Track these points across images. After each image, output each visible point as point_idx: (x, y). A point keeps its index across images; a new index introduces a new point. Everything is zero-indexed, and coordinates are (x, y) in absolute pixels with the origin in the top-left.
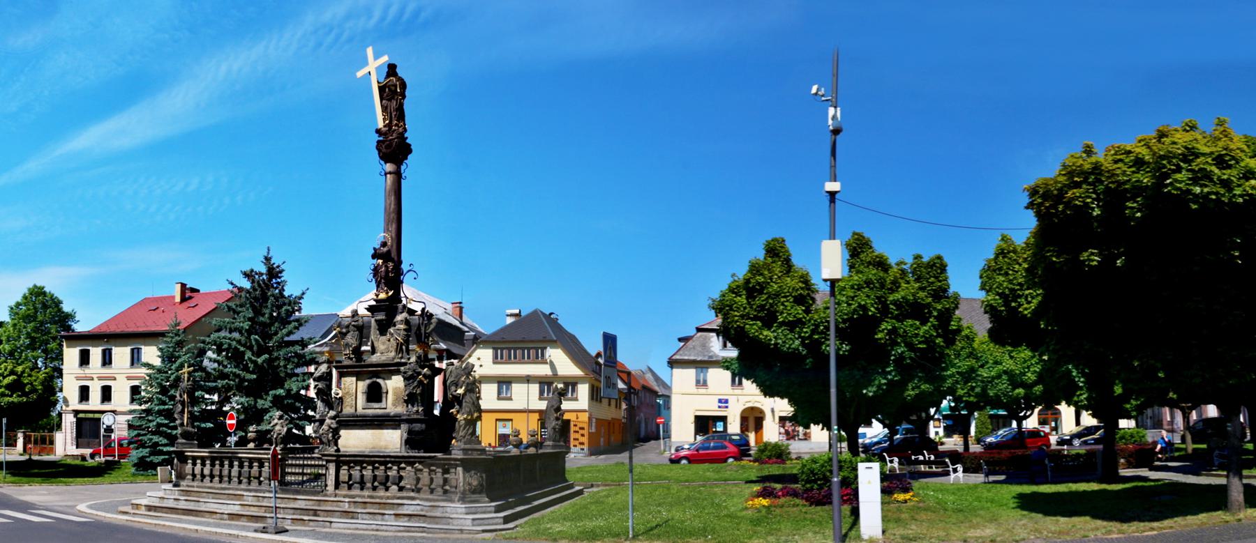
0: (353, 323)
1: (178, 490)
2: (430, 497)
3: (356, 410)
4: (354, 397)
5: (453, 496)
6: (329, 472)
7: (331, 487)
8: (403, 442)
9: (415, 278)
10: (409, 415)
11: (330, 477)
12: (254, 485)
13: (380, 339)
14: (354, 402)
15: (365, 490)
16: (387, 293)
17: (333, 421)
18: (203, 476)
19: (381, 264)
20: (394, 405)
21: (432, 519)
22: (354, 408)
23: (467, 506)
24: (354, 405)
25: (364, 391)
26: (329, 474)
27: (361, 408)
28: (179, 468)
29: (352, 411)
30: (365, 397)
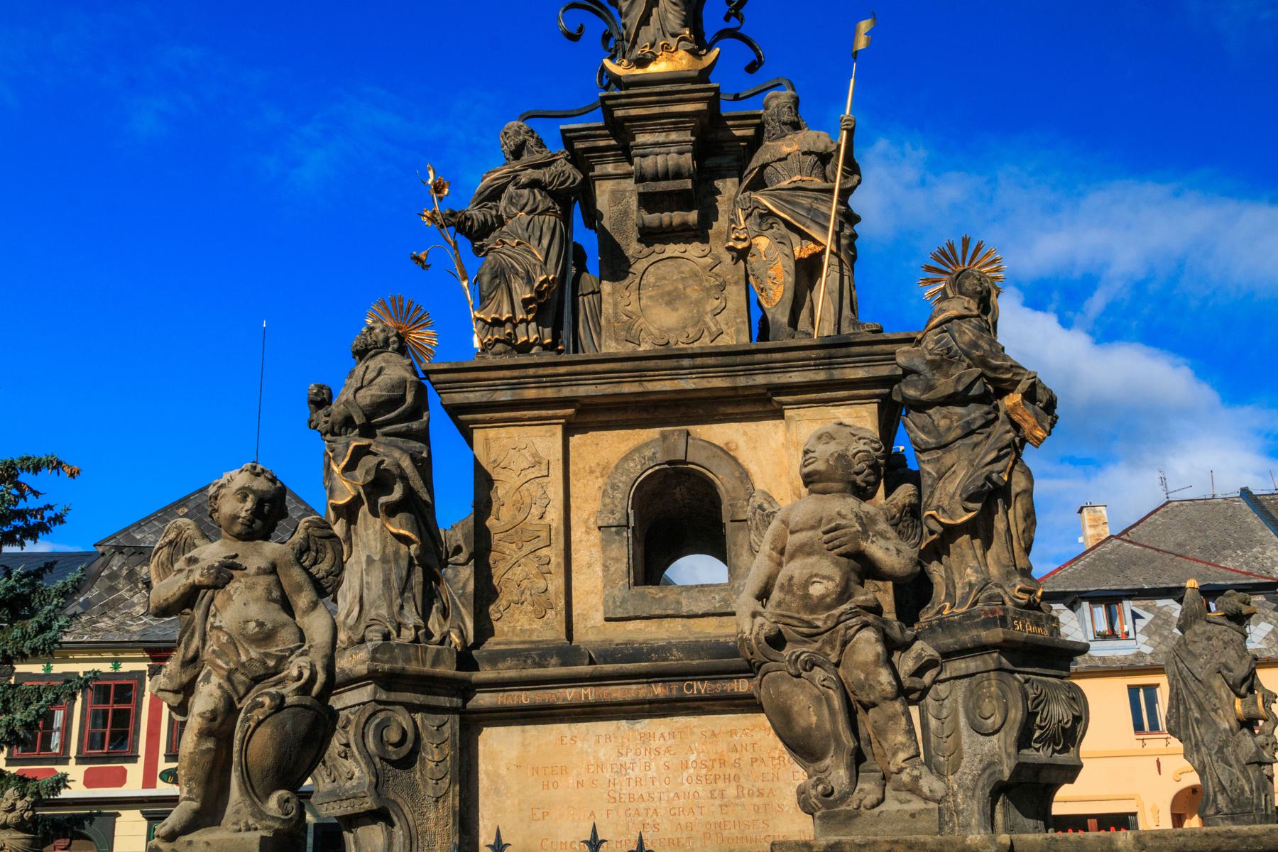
3: (569, 635)
4: (554, 554)
13: (650, 278)
14: (557, 583)
24: (562, 603)
25: (618, 517)
27: (598, 618)
29: (549, 630)
30: (621, 552)
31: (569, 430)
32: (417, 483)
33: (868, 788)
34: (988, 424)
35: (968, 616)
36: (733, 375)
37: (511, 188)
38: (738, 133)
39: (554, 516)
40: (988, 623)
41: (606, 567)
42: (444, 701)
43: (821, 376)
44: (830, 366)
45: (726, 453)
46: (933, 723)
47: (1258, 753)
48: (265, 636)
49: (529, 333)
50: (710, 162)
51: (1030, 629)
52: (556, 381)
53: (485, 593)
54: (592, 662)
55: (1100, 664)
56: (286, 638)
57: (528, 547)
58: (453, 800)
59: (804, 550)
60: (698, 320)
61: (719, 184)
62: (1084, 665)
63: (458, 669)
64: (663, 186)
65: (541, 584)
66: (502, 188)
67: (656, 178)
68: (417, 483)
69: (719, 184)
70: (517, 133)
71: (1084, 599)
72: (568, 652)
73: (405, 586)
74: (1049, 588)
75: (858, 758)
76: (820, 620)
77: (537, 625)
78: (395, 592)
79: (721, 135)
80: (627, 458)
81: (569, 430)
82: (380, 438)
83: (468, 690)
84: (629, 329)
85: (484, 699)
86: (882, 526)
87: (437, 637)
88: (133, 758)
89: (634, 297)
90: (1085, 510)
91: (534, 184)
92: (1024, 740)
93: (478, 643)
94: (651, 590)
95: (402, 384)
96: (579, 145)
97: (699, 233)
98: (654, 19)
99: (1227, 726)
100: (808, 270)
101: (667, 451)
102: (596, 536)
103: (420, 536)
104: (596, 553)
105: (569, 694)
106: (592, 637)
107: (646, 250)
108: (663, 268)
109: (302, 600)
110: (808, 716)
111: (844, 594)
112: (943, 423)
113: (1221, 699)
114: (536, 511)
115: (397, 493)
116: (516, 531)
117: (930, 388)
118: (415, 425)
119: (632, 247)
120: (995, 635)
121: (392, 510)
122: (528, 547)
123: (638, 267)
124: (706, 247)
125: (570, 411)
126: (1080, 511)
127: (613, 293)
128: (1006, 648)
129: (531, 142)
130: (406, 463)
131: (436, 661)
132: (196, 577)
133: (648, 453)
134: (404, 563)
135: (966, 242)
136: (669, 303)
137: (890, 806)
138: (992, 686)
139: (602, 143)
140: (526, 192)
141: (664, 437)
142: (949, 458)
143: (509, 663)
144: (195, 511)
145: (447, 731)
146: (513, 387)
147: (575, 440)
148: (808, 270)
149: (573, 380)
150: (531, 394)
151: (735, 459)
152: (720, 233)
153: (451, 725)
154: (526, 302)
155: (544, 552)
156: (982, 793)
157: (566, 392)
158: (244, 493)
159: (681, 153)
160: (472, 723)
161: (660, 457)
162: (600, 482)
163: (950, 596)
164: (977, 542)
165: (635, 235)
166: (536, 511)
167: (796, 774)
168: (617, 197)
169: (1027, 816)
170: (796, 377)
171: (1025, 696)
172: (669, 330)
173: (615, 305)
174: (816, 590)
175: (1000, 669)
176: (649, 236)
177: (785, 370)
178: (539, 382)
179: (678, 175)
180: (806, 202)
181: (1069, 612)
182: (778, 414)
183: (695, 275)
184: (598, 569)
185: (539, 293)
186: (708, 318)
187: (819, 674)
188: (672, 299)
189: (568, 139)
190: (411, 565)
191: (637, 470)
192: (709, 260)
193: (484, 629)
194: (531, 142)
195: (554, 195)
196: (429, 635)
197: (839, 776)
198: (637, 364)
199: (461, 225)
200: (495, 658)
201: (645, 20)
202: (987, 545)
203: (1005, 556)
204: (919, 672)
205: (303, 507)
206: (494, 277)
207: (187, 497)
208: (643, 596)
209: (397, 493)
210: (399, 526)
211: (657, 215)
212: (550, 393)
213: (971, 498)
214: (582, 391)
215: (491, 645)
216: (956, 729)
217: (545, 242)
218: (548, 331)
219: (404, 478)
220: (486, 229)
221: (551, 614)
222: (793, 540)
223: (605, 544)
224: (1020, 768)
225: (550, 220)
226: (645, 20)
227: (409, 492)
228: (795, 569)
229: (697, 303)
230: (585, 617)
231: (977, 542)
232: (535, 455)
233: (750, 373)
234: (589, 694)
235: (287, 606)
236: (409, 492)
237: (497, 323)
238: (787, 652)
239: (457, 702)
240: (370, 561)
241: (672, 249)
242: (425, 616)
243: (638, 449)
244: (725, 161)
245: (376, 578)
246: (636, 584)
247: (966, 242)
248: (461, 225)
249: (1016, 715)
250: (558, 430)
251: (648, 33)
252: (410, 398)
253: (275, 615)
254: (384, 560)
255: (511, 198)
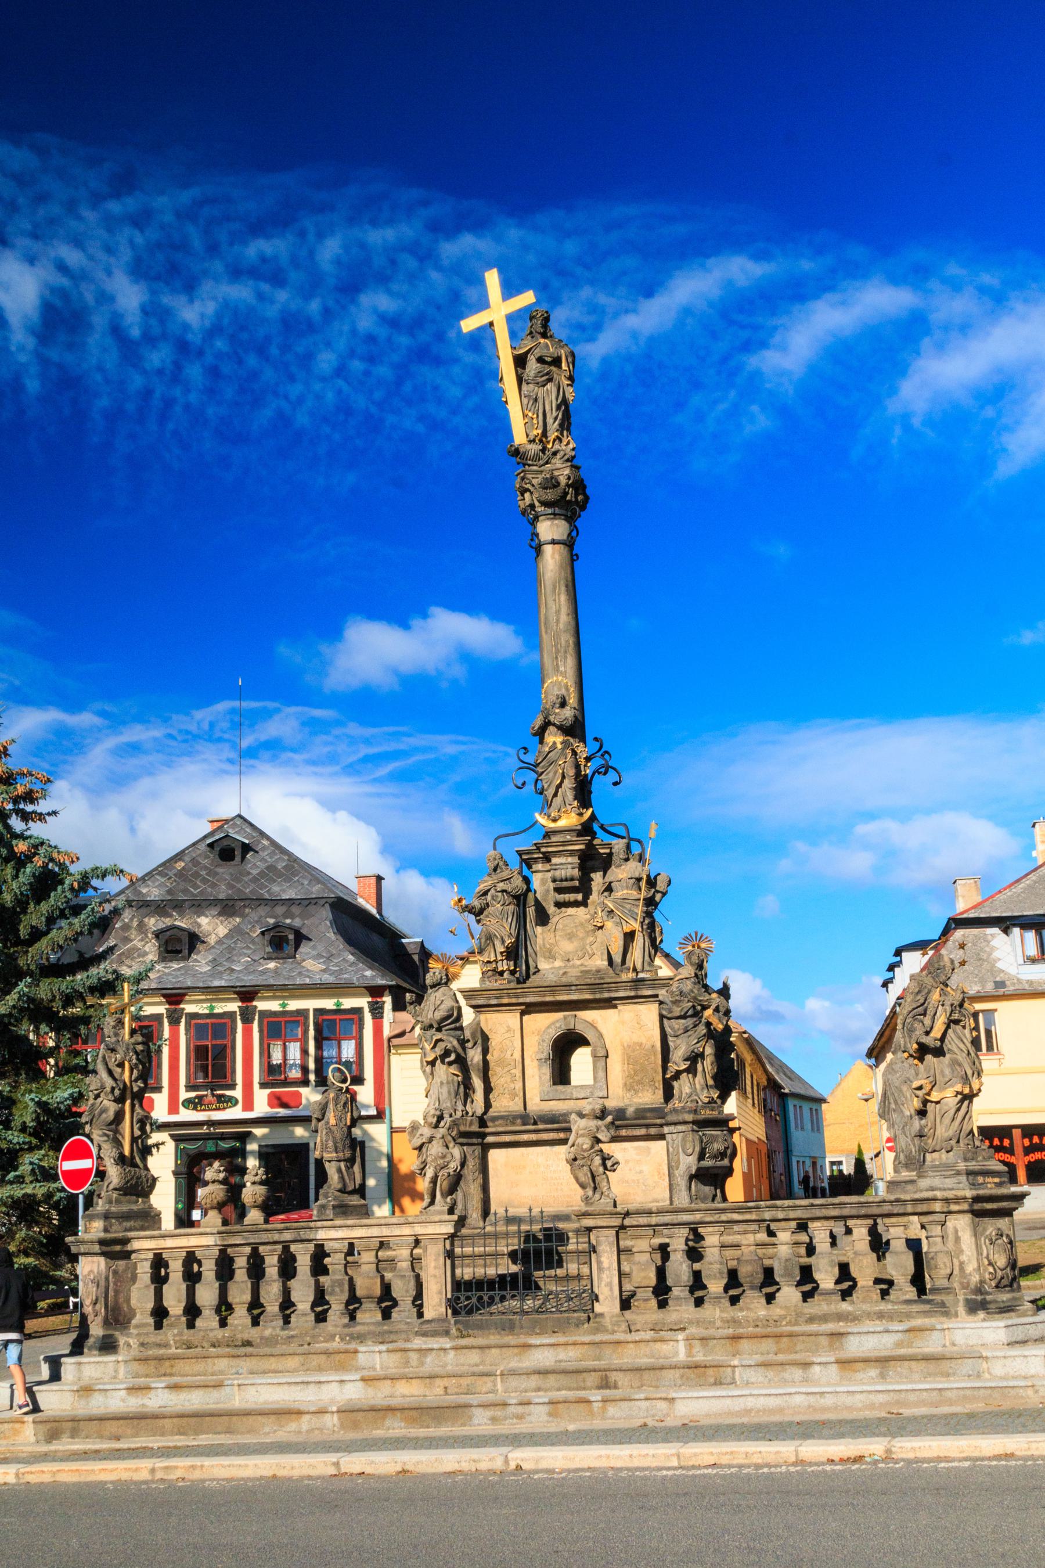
0: (501, 886)
1: (126, 1362)
2: (883, 1306)
4: (518, 1072)
5: (947, 1299)
6: (599, 1262)
7: (608, 1305)
8: (682, 1182)
9: (616, 784)
10: (695, 1111)
11: (604, 1276)
12: (369, 1316)
13: (560, 926)
15: (706, 1305)
16: (581, 814)
17: (600, 1123)
18: (192, 1311)
19: (559, 746)
20: (629, 1087)
21: (932, 1366)
22: (519, 1101)
23: (1010, 1322)
25: (545, 1055)
26: (600, 1269)
27: (537, 1100)
28: (111, 1293)
29: (516, 1106)
30: (547, 1071)
31: (523, 1013)
32: (460, 1050)
33: (597, 1196)
34: (695, 1026)
35: (683, 1108)
36: (594, 993)
37: (492, 891)
38: (602, 851)
39: (517, 1055)
40: (690, 1112)
41: (540, 1078)
42: (475, 1141)
43: (632, 994)
44: (636, 989)
45: (593, 1026)
46: (671, 1149)
47: (920, 1131)
48: (444, 1157)
49: (504, 966)
50: (589, 864)
51: (708, 1112)
52: (517, 997)
53: (488, 1089)
54: (535, 1123)
55: (1027, 987)
56: (449, 1157)
57: (506, 1069)
58: (480, 1181)
59: (583, 1135)
60: (583, 948)
61: (593, 875)
62: (1012, 988)
63: (480, 1127)
64: (565, 884)
65: (512, 1086)
66: (489, 890)
67: (561, 880)
68: (460, 1050)
69: (593, 875)
70: (495, 859)
71: (1015, 925)
72: (525, 1118)
73: (457, 1094)
74: (986, 912)
75: (595, 1189)
76: (586, 1154)
77: (511, 1103)
78: (453, 1095)
79: (593, 852)
80: (548, 1028)
81: (523, 1013)
82: (444, 1032)
83: (484, 1135)
84: (550, 952)
85: (490, 1139)
86: (603, 1128)
87: (470, 1114)
88: (158, 1089)
89: (552, 935)
90: (1037, 825)
91: (503, 891)
92: (701, 1157)
93: (485, 1113)
94: (560, 1088)
95: (452, 1009)
96: (524, 857)
97: (584, 903)
98: (559, 794)
99: (908, 1113)
100: (629, 937)
101: (566, 1025)
102: (536, 1063)
103: (462, 1073)
104: (536, 1070)
105: (525, 1137)
106: (535, 1108)
107: (558, 911)
108: (567, 921)
109: (451, 1145)
110: (583, 1179)
111: (592, 1147)
112: (676, 1027)
113: (906, 1098)
114: (509, 1053)
115: (453, 1057)
116: (501, 1062)
117: (670, 1012)
118: (458, 1025)
119: (551, 909)
120: (689, 1117)
121: (450, 1064)
122: (506, 1069)
123: (553, 920)
124: (586, 910)
125: (523, 1007)
126: (1034, 826)
127: (542, 934)
128: (694, 1122)
129: (501, 864)
130: (455, 1043)
131: (471, 1124)
132: (424, 1140)
133: (558, 1025)
134: (456, 1084)
135: (696, 934)
136: (569, 939)
137: (602, 1200)
138: (690, 1136)
139: (536, 856)
140: (500, 894)
141: (565, 1018)
142: (678, 1042)
143: (500, 1122)
144: (190, 865)
145: (476, 1153)
146: (497, 998)
147: (526, 1018)
148: (629, 937)
149: (524, 995)
150: (505, 1001)
151: (596, 1028)
152: (594, 902)
153: (478, 1150)
154: (502, 953)
155: (513, 1071)
156: (686, 1178)
157: (521, 1000)
158: (434, 1116)
159: (573, 868)
160: (486, 1148)
161: (563, 1027)
162: (537, 1038)
163: (680, 1098)
164: (690, 1075)
165: (552, 904)
166: (509, 1053)
167: (580, 1191)
168: (543, 882)
169: (705, 1185)
170: (621, 994)
171: (701, 1141)
172: (569, 953)
173: (544, 939)
174: (585, 1147)
175: (693, 1131)
176: (559, 905)
177: (617, 991)
178: (509, 997)
179: (572, 879)
180: (628, 906)
181: (1003, 935)
182: (615, 1007)
183: (582, 924)
184: (537, 1078)
185: (507, 948)
186: (588, 947)
187: (585, 1168)
188: (570, 937)
189: (520, 853)
190: (459, 1085)
191: (554, 1033)
192: (588, 916)
193: (488, 1105)
194: (501, 864)
195: (515, 897)
196: (467, 1113)
197: (590, 1193)
198: (553, 988)
199: (469, 909)
200: (494, 1119)
201: (555, 795)
202: (695, 1075)
203: (702, 1081)
204: (613, 1165)
205: (286, 858)
206: (487, 939)
207: (183, 851)
208: (556, 1091)
209: (453, 1057)
210: (454, 1069)
211: (562, 896)
212: (514, 1001)
213: (686, 1060)
214: (528, 1000)
215: (492, 1113)
216: (678, 1153)
217: (510, 920)
218: (512, 963)
219: (455, 1051)
220: (481, 911)
221: (517, 1099)
222: (581, 1132)
223: (540, 1067)
224: (699, 1169)
225: (511, 908)
226: (555, 795)
227: (458, 1056)
228: (580, 1140)
229: (582, 939)
230: (531, 1099)
231: (690, 1075)
232: (508, 1027)
233: (601, 992)
234: (533, 1137)
235: (447, 1147)
236: (458, 1056)
237: (488, 962)
238: (577, 1163)
239: (480, 1140)
240: (442, 1083)
241: (571, 911)
242: (465, 1105)
243: (553, 1023)
244: (597, 863)
245: (445, 1090)
246: (554, 1084)
247: (696, 934)
248: (469, 909)
249: (697, 1149)
250: (518, 1015)
251: (558, 800)
252: (455, 1014)
253: (445, 1150)
254: (448, 1083)
255: (493, 897)
